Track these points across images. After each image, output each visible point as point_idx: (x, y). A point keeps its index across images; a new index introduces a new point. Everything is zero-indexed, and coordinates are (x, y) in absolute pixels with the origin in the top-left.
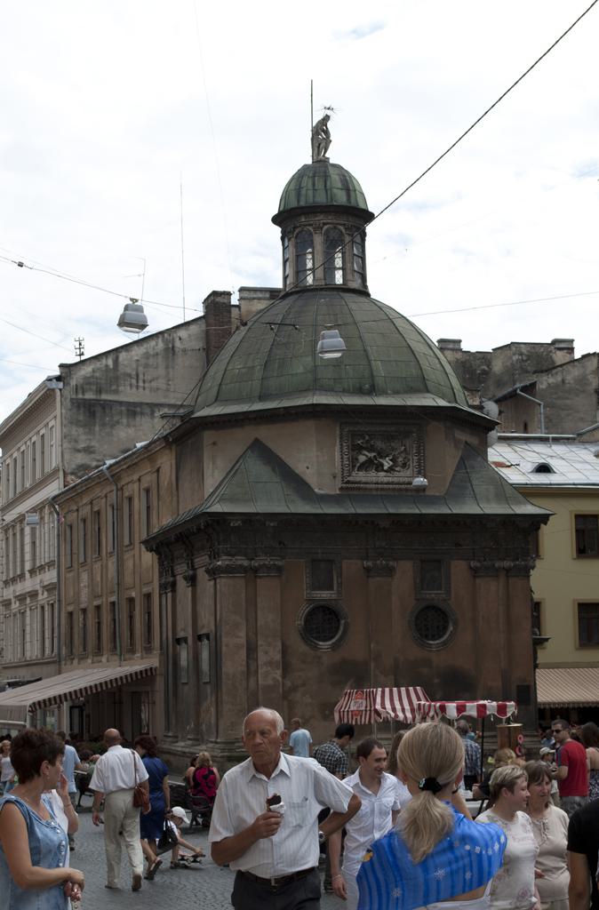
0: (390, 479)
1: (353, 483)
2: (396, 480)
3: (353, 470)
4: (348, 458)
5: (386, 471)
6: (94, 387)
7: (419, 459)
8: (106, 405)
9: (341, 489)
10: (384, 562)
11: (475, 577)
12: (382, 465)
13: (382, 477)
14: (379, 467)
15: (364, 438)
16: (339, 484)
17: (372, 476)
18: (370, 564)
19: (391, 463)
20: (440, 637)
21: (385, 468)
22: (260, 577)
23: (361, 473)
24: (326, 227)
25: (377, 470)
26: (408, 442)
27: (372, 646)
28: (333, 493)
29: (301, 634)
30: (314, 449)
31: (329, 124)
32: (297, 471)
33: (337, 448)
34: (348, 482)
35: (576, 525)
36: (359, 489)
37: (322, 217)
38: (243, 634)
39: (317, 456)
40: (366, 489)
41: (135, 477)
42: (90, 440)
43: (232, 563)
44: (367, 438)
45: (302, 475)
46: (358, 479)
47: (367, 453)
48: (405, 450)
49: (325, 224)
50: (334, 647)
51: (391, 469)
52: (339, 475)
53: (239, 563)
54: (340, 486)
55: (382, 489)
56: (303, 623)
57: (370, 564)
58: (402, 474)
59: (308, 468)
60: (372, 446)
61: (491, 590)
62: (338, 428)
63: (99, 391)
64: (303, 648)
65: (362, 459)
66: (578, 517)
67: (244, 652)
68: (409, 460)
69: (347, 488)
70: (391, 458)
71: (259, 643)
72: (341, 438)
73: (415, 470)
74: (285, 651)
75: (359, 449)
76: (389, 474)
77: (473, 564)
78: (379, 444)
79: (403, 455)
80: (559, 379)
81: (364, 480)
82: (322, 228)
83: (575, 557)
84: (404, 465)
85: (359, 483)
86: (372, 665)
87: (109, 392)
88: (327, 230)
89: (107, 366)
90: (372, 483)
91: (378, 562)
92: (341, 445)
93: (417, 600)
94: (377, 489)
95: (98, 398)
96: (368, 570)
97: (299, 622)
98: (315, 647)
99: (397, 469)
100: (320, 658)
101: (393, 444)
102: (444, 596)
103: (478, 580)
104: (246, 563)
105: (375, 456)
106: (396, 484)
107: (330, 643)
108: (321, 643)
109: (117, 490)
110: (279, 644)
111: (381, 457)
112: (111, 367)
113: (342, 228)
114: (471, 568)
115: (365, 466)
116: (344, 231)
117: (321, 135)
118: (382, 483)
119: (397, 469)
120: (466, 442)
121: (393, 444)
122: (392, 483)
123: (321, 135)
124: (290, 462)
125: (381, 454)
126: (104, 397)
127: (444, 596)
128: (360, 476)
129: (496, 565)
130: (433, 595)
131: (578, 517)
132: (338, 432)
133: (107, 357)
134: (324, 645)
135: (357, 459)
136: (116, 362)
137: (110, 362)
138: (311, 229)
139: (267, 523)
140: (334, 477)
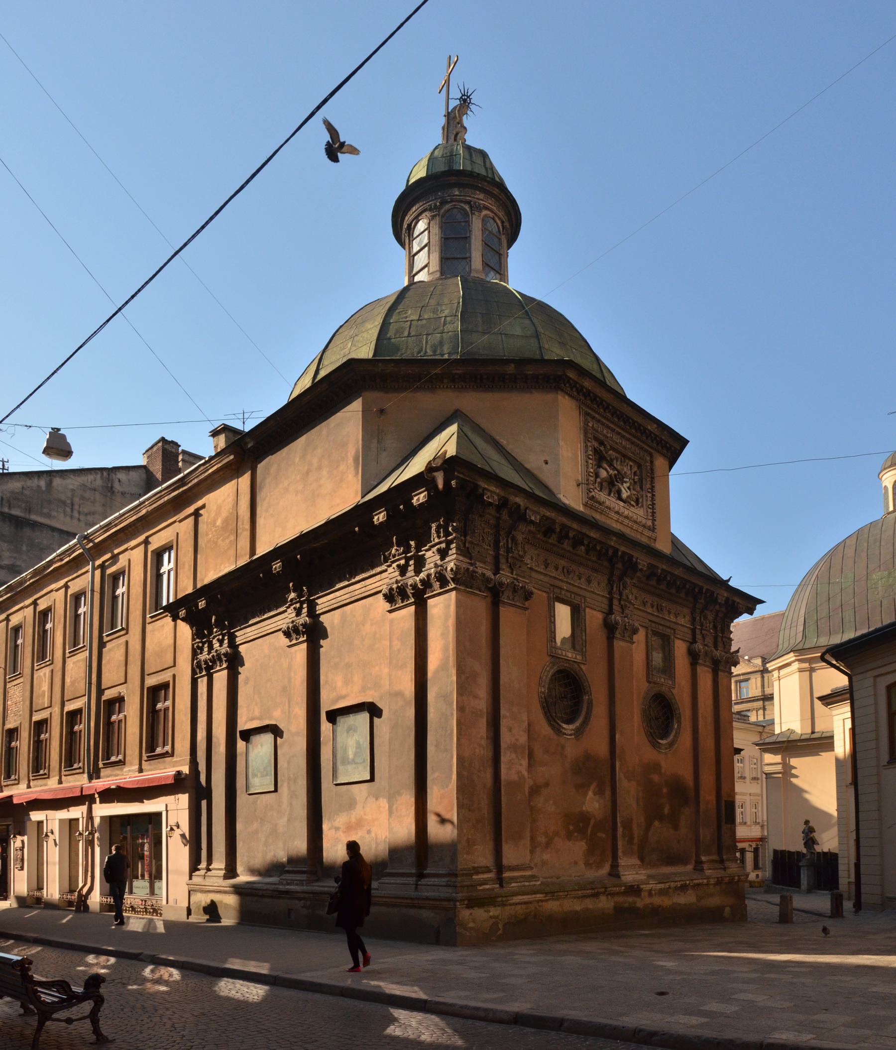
6: (23, 505)
8: (34, 525)
41: (142, 538)
42: (15, 558)
50: (579, 733)
63: (30, 510)
87: (42, 515)
89: (39, 486)
95: (27, 516)
98: (558, 731)
100: (563, 747)
108: (565, 726)
109: (94, 569)
112: (44, 488)
126: (33, 517)
133: (39, 477)
134: (569, 728)
136: (49, 484)
137: (43, 483)
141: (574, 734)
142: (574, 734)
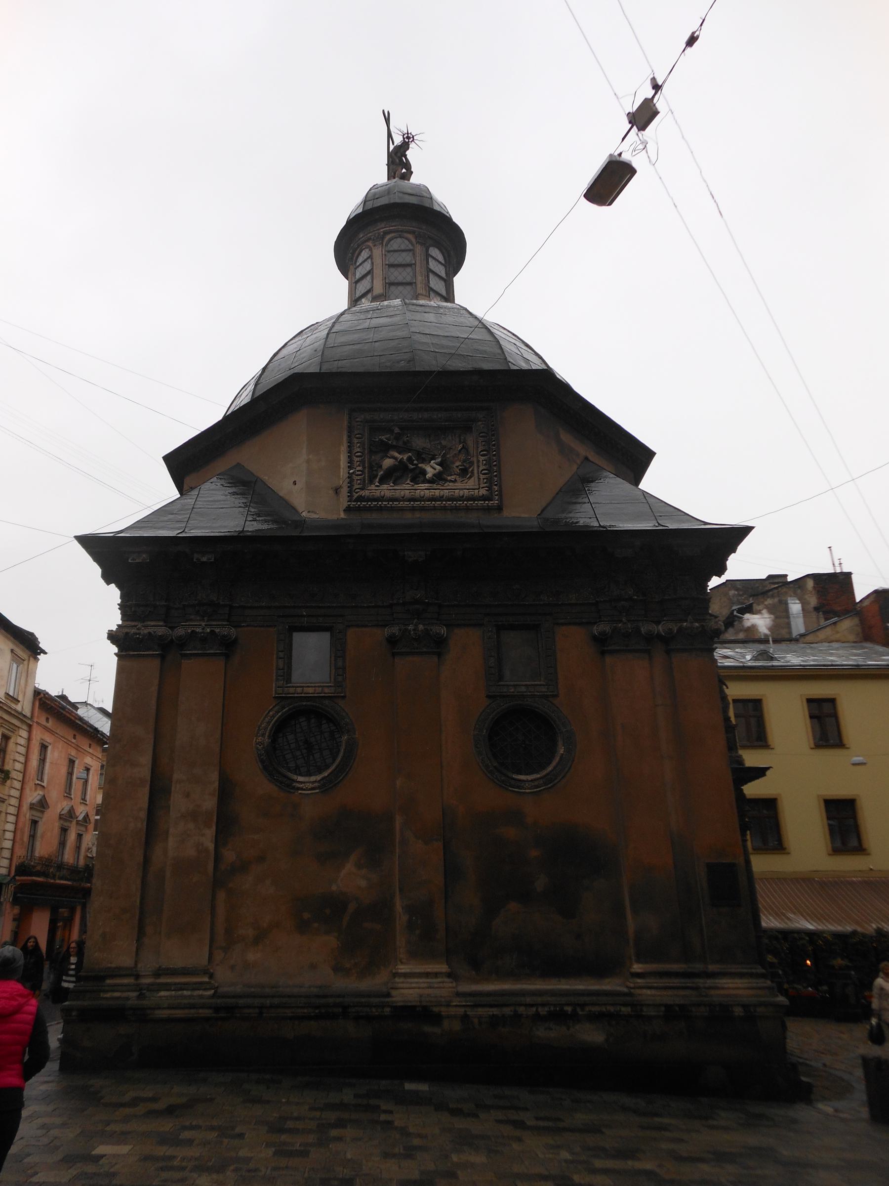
0: (437, 492)
1: (369, 499)
2: (446, 493)
3: (371, 482)
4: (362, 462)
5: (430, 481)
7: (489, 462)
9: (348, 510)
10: (421, 627)
11: (603, 653)
12: (424, 473)
13: (422, 490)
14: (418, 476)
15: (391, 431)
16: (344, 502)
17: (405, 489)
18: (395, 630)
19: (438, 468)
20: (544, 768)
21: (429, 476)
22: (185, 655)
23: (385, 486)
24: (388, 237)
25: (414, 480)
26: (470, 441)
27: (398, 783)
28: (335, 517)
29: (262, 761)
30: (304, 451)
31: (409, 154)
32: (281, 494)
33: (344, 448)
34: (360, 499)
35: (809, 710)
36: (380, 509)
37: (383, 225)
38: (146, 760)
39: (308, 461)
40: (392, 509)
43: (133, 631)
44: (397, 430)
45: (287, 498)
46: (377, 494)
47: (396, 455)
48: (463, 447)
49: (386, 233)
50: (326, 786)
51: (439, 478)
52: (345, 491)
53: (151, 630)
54: (346, 504)
55: (423, 509)
56: (267, 740)
57: (395, 630)
58: (459, 485)
59: (295, 483)
60: (405, 443)
61: (635, 678)
62: (346, 417)
64: (263, 786)
65: (388, 463)
66: (810, 701)
67: (144, 794)
68: (472, 463)
69: (359, 509)
70: (439, 460)
71: (176, 776)
72: (350, 430)
73: (482, 477)
74: (226, 791)
75: (385, 448)
76: (435, 486)
77: (596, 630)
78: (419, 442)
79: (462, 457)
80: (776, 600)
81: (388, 494)
82: (383, 238)
83: (813, 746)
84: (464, 472)
85: (382, 499)
86: (399, 821)
88: (390, 240)
90: (403, 499)
91: (411, 627)
92: (350, 441)
93: (488, 697)
94: (413, 509)
96: (392, 641)
97: (260, 739)
98: (288, 786)
99: (449, 478)
101: (444, 443)
102: (544, 689)
103: (609, 659)
104: (161, 631)
105: (409, 459)
106: (448, 499)
107: (319, 777)
108: (300, 779)
110: (214, 776)
111: (423, 461)
113: (410, 236)
114: (595, 639)
115: (394, 475)
116: (413, 240)
117: (398, 161)
118: (422, 499)
119: (449, 478)
120: (586, 458)
121: (444, 443)
122: (441, 499)
123: (398, 161)
124: (273, 482)
125: (423, 456)
127: (544, 689)
128: (386, 490)
129: (643, 630)
130: (523, 689)
131: (810, 701)
132: (346, 423)
135: (381, 467)
138: (370, 244)
139: (196, 556)
140: (337, 491)
141: (319, 788)
142: (319, 788)
